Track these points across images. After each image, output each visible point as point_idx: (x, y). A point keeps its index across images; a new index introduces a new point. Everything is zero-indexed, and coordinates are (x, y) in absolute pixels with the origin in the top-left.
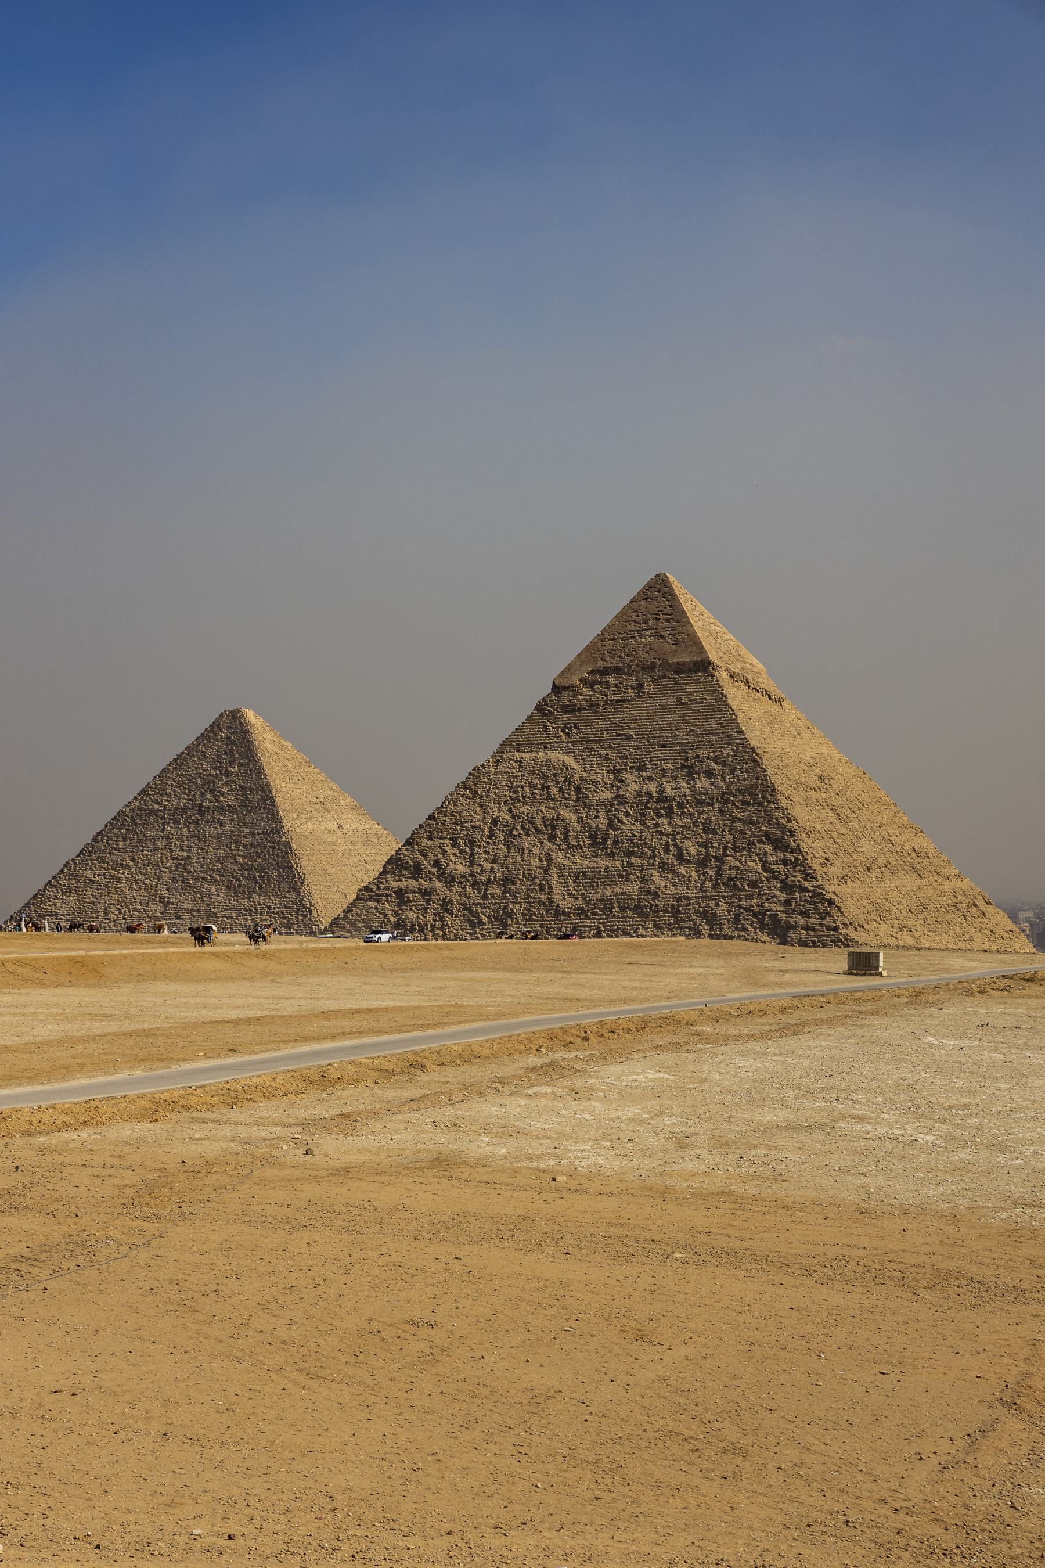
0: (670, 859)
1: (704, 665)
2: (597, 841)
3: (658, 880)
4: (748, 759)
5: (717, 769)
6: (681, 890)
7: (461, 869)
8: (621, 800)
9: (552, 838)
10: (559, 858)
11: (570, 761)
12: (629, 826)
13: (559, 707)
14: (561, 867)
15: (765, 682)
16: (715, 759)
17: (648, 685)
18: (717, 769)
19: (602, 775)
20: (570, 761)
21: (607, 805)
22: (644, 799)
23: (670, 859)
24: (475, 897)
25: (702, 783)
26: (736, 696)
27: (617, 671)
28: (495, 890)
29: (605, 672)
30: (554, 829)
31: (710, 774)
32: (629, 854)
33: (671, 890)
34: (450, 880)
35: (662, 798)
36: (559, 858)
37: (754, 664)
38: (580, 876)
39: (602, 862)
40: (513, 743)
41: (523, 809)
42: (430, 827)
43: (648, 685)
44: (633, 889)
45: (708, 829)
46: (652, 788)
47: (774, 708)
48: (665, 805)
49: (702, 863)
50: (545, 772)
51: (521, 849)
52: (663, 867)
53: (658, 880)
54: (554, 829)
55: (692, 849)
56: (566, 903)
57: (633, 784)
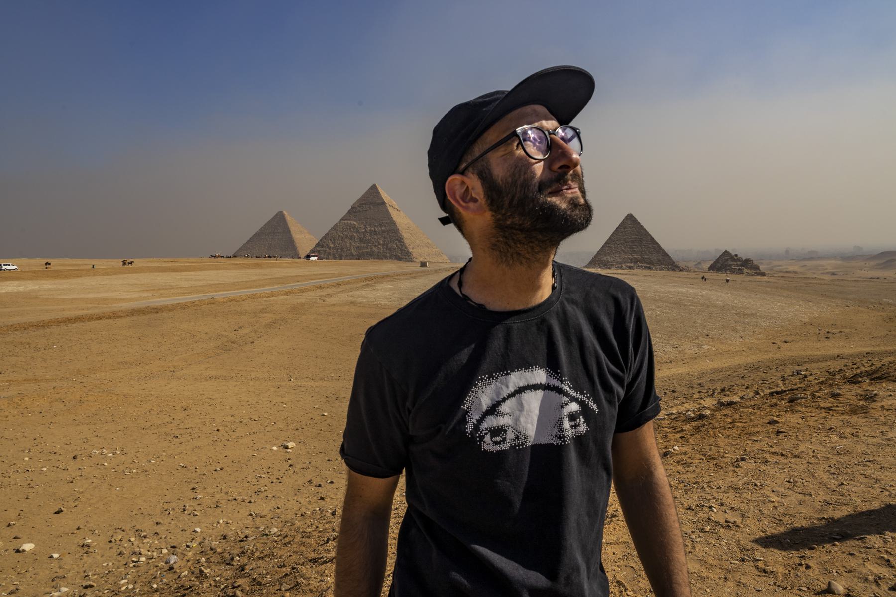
1: (384, 203)
2: (361, 240)
4: (393, 223)
12: (368, 237)
13: (353, 212)
19: (362, 226)
22: (371, 232)
26: (390, 210)
30: (352, 238)
34: (330, 248)
35: (375, 231)
37: (394, 203)
40: (343, 219)
42: (326, 237)
44: (369, 250)
48: (375, 233)
49: (383, 245)
54: (352, 238)
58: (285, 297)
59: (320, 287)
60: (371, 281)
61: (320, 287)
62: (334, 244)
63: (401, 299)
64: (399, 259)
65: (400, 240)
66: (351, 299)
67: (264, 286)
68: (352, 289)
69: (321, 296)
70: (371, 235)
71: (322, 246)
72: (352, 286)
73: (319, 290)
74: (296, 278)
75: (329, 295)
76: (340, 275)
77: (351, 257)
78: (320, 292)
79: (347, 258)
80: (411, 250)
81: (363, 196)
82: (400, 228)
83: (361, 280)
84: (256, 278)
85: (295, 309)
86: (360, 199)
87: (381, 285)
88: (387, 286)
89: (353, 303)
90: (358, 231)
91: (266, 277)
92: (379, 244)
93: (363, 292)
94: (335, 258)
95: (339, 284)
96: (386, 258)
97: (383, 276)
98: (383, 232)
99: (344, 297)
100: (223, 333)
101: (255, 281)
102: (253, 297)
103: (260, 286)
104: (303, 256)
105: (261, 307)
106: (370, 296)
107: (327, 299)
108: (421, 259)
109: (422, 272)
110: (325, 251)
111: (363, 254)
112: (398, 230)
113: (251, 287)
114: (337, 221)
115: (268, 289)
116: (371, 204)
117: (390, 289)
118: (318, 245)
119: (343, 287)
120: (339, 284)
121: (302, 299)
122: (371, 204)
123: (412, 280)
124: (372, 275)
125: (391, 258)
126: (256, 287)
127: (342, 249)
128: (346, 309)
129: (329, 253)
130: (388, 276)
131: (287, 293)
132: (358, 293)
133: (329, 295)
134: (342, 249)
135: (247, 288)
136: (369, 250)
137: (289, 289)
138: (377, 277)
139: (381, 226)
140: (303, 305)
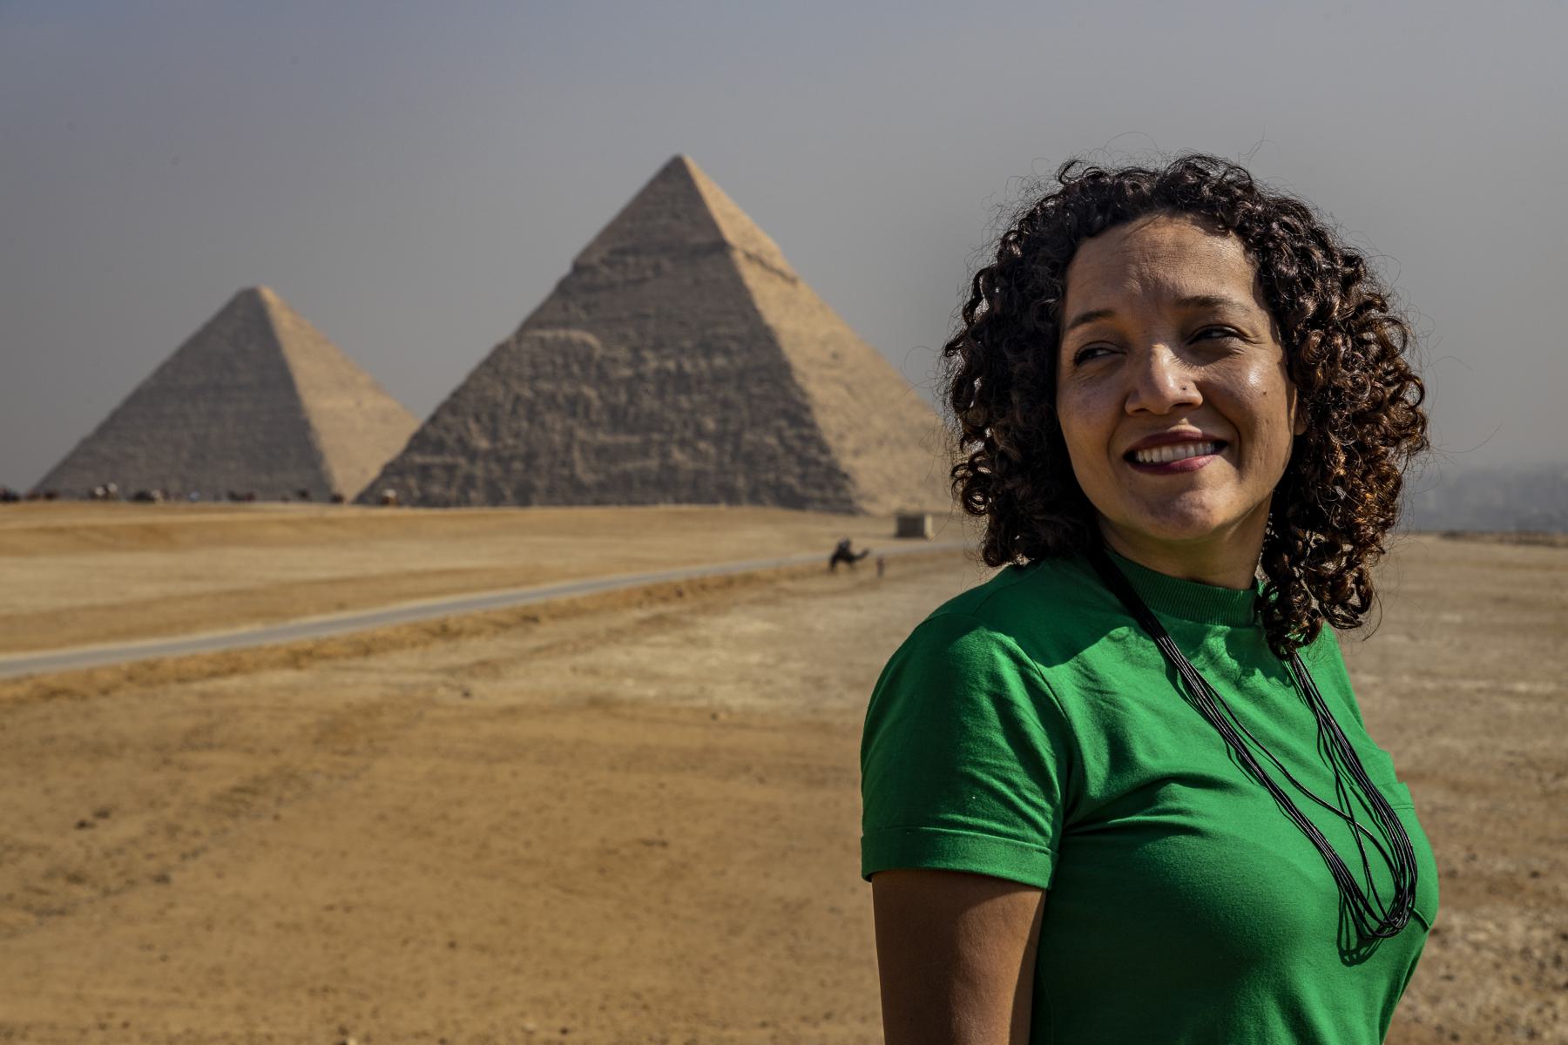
0: (689, 434)
1: (721, 247)
2: (618, 418)
3: (678, 456)
4: (763, 337)
5: (734, 346)
7: (484, 444)
8: (640, 377)
9: (574, 414)
10: (581, 434)
11: (591, 339)
12: (649, 403)
13: (580, 287)
14: (583, 444)
15: (779, 262)
16: (734, 338)
17: (667, 265)
18: (734, 346)
19: (622, 353)
20: (591, 339)
21: (628, 382)
22: (662, 375)
23: (689, 434)
24: (497, 470)
25: (720, 361)
26: (752, 276)
27: (636, 251)
28: (518, 466)
29: (623, 252)
30: (575, 407)
31: (727, 352)
33: (691, 465)
34: (473, 455)
35: (681, 374)
36: (581, 434)
37: (768, 244)
38: (601, 451)
39: (623, 439)
40: (535, 321)
41: (546, 386)
42: (453, 405)
43: (667, 265)
44: (653, 463)
45: (726, 404)
46: (671, 365)
47: (787, 288)
48: (681, 382)
49: (718, 439)
50: (566, 349)
51: (543, 425)
52: (683, 443)
53: (678, 456)
54: (575, 407)
55: (710, 424)
56: (588, 478)
57: (652, 362)
58: (289, 676)
59: (444, 632)
60: (676, 601)
61: (444, 632)
62: (494, 436)
63: (819, 683)
64: (793, 501)
65: (798, 413)
66: (589, 685)
67: (188, 626)
68: (588, 641)
69: (452, 671)
70: (661, 393)
71: (440, 447)
72: (587, 624)
73: (439, 646)
74: (334, 593)
75: (487, 667)
76: (531, 576)
77: (573, 493)
78: (443, 655)
79: (553, 497)
80: (847, 462)
81: (628, 214)
82: (796, 357)
83: (629, 599)
84: (149, 590)
85: (338, 731)
86: (613, 230)
87: (723, 622)
88: (751, 623)
89: (600, 704)
90: (603, 378)
91: (195, 587)
92: (700, 434)
93: (644, 654)
94: (495, 498)
95: (529, 619)
96: (730, 496)
97: (728, 583)
98: (719, 378)
99: (552, 678)
100: (26, 836)
101: (146, 605)
102: (146, 676)
103: (169, 628)
104: (350, 493)
105: (187, 723)
106: (675, 669)
107: (480, 686)
108: (896, 503)
109: (905, 559)
110: (450, 469)
111: (627, 479)
112: (784, 369)
113: (130, 633)
114: (504, 328)
115: (208, 640)
116: (663, 246)
117: (766, 640)
118: (419, 441)
119: (547, 631)
120: (529, 619)
121: (363, 684)
122: (663, 246)
123: (861, 599)
124: (679, 574)
125: (755, 498)
126: (155, 631)
127: (530, 458)
128: (569, 729)
129: (469, 481)
130: (748, 580)
131: (295, 659)
132: (618, 656)
133: (487, 667)
134: (530, 458)
135: (113, 635)
136: (653, 463)
137: (305, 641)
138: (701, 587)
139: (707, 349)
140: (371, 711)
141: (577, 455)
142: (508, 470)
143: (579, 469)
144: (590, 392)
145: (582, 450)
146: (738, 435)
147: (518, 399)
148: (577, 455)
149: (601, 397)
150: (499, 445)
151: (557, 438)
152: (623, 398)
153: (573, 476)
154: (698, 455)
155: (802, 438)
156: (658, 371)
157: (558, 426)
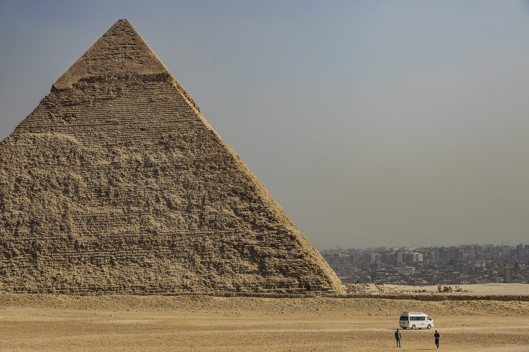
3: (155, 223)
6: (173, 229)
9: (66, 192)
10: (73, 206)
12: (124, 184)
28: (24, 230)
30: (66, 186)
32: (128, 203)
35: (148, 164)
36: (73, 206)
38: (91, 219)
39: (107, 210)
44: (135, 228)
46: (139, 157)
54: (66, 186)
56: (82, 240)
90: (85, 164)
141: (71, 221)
142: (16, 235)
143: (74, 235)
144: (78, 177)
145: (76, 219)
146: (201, 207)
147: (19, 180)
148: (71, 221)
149: (86, 179)
150: (7, 214)
151: (54, 210)
152: (104, 181)
153: (70, 238)
154: (170, 223)
155: (251, 209)
156: (129, 162)
157: (54, 201)
